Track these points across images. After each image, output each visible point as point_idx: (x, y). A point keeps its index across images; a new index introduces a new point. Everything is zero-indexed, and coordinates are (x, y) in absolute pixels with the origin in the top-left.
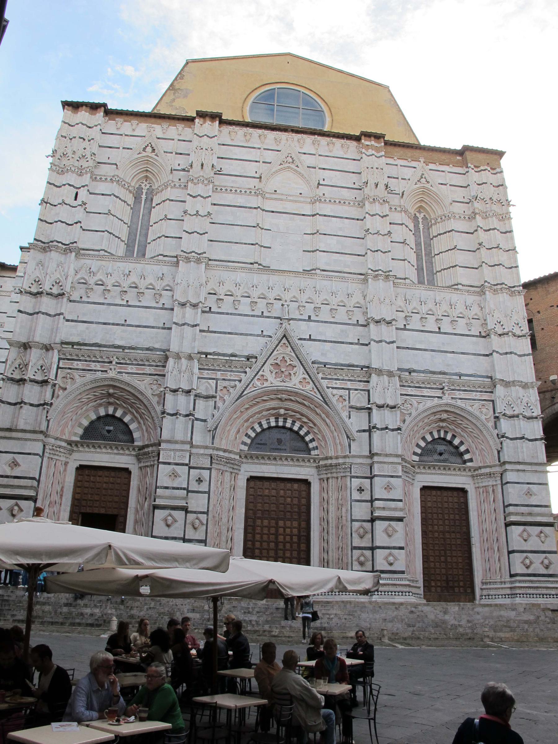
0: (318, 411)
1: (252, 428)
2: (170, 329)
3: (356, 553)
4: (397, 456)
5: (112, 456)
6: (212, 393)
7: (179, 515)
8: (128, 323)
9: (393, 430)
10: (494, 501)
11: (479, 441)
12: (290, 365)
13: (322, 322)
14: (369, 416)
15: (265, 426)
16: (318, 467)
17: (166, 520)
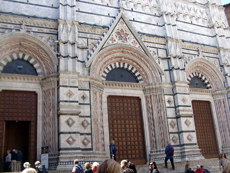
0: (143, 59)
1: (107, 68)
2: (57, 8)
3: (172, 136)
4: (186, 83)
5: (24, 84)
6: (85, 45)
7: (74, 118)
8: (29, 2)
9: (181, 70)
10: (224, 107)
11: (214, 77)
12: (126, 33)
13: (139, 12)
14: (168, 62)
15: (114, 67)
16: (144, 90)
17: (67, 122)
